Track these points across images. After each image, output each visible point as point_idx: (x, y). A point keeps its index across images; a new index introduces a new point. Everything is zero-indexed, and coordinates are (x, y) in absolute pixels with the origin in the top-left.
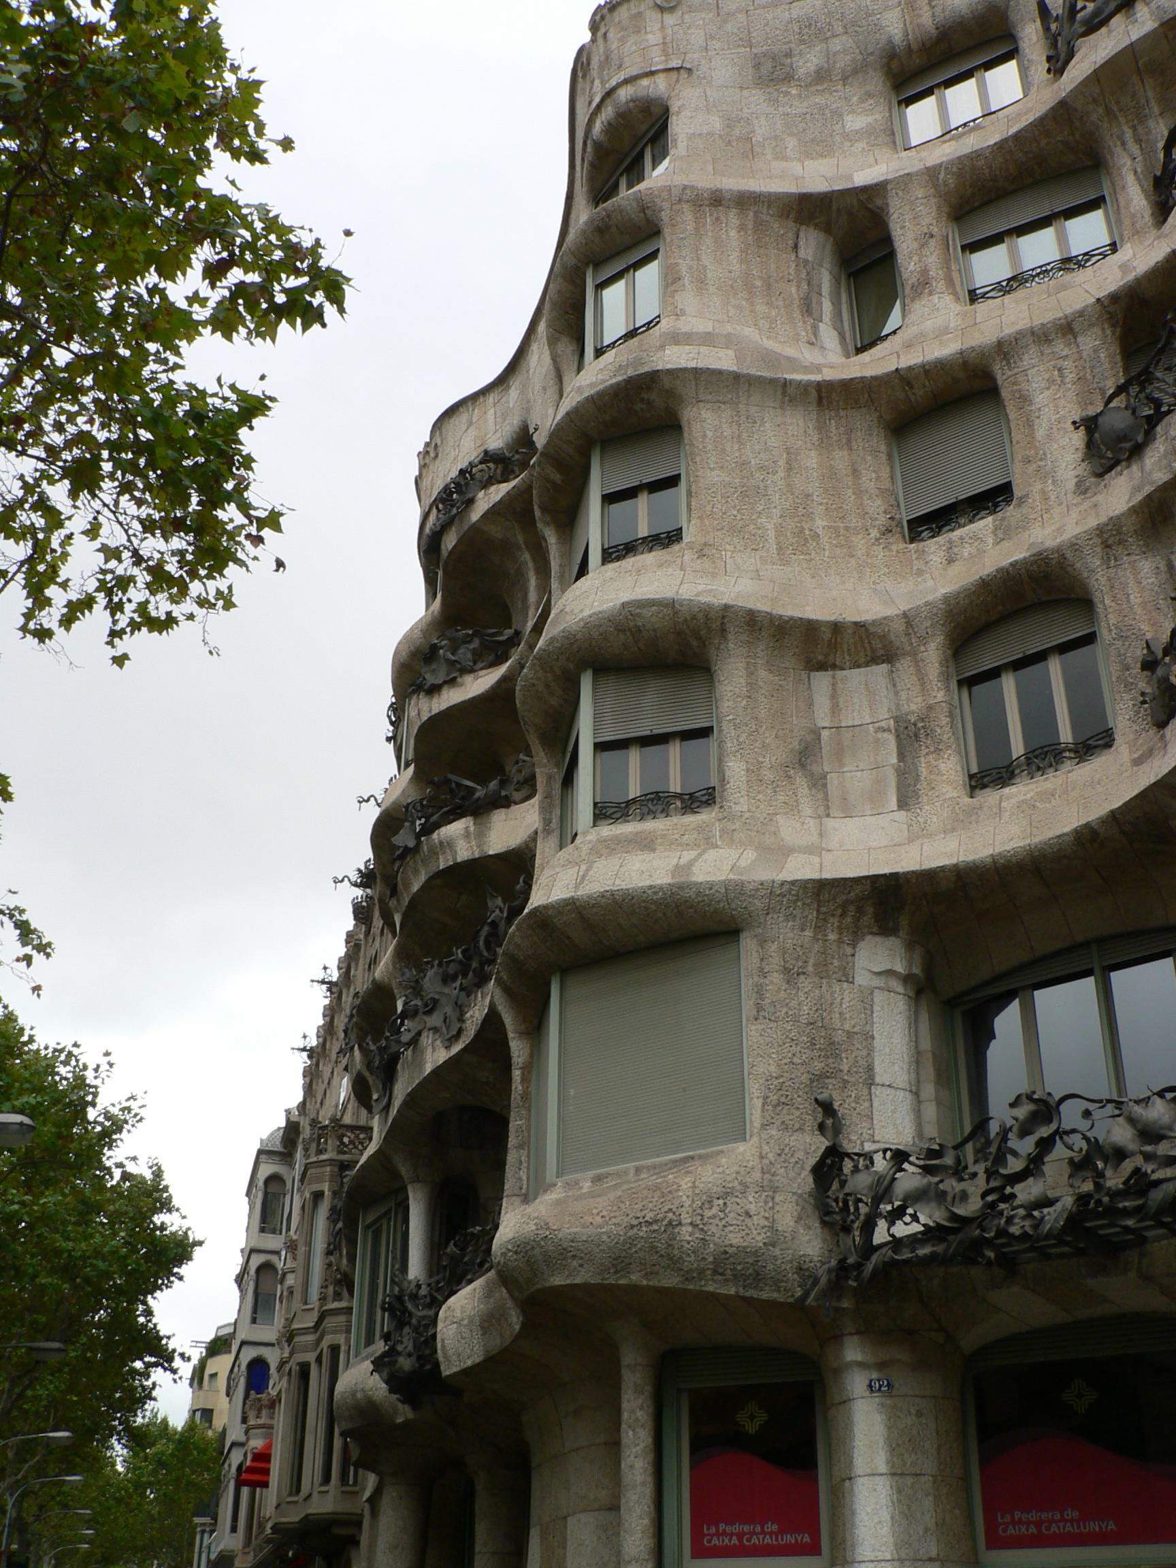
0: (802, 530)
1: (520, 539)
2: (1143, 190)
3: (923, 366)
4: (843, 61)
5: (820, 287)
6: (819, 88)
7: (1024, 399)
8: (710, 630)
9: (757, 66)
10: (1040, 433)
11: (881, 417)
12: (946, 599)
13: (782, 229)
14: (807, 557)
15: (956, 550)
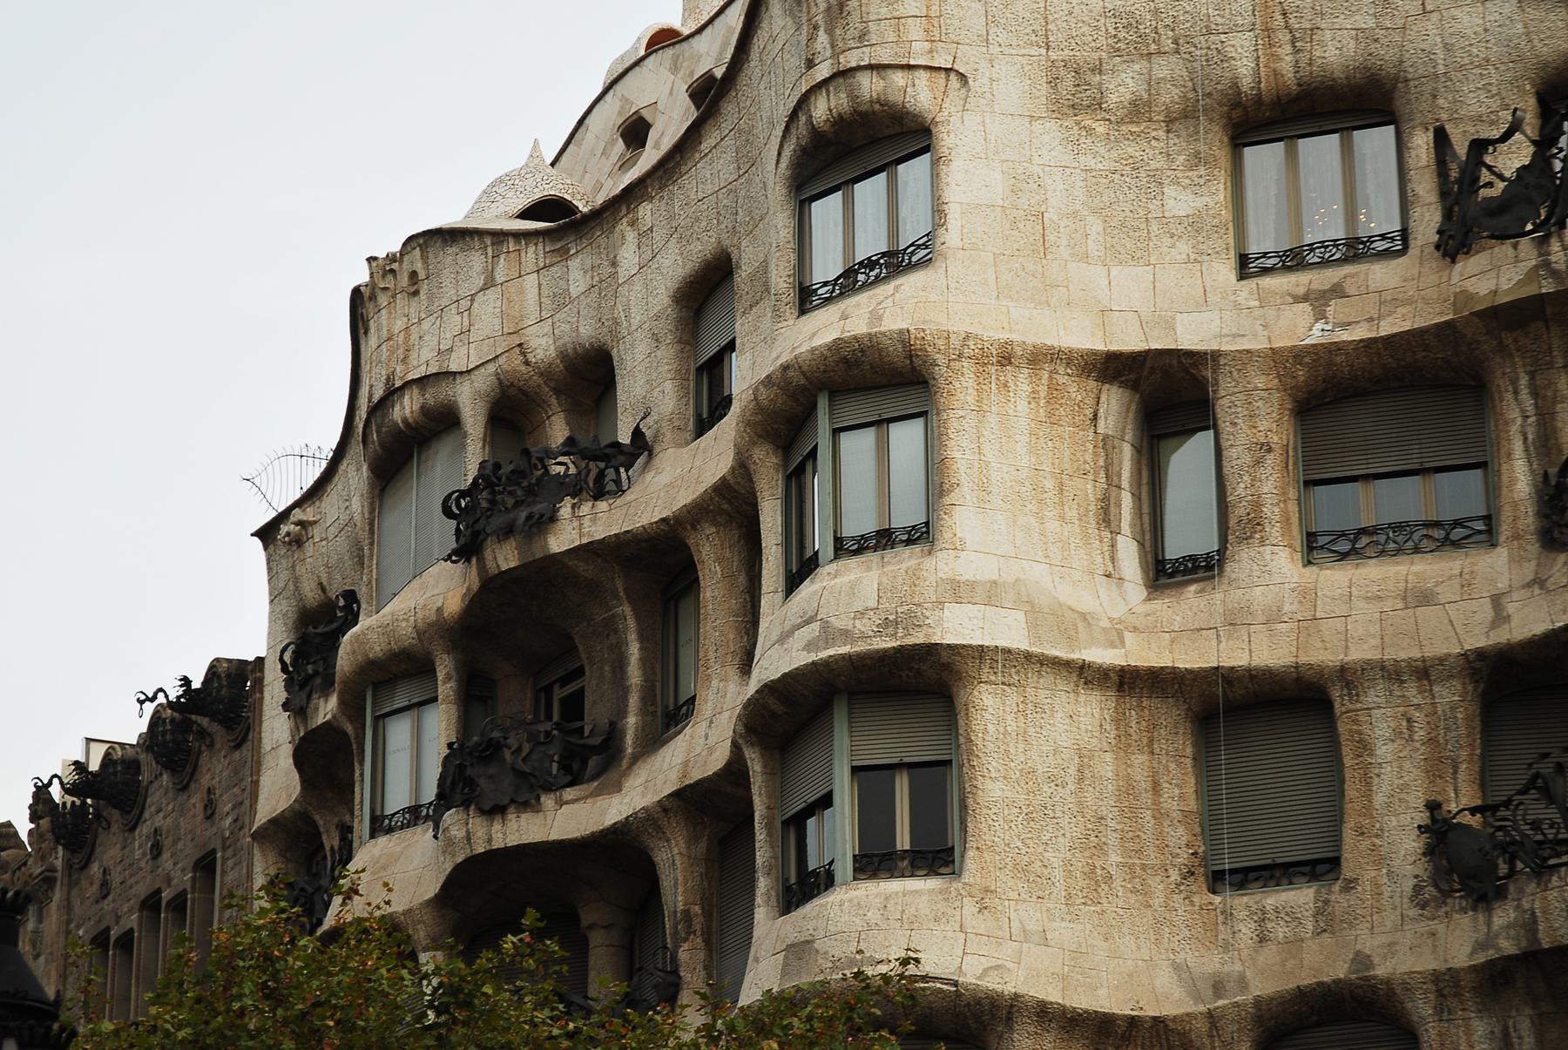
0: (1093, 871)
1: (619, 585)
2: (1532, 471)
3: (1249, 670)
4: (1170, 95)
5: (1119, 475)
6: (1135, 129)
7: (1364, 747)
8: (993, 1017)
9: (1054, 82)
10: (1379, 799)
11: (1189, 709)
12: (1258, 1002)
13: (1077, 390)
14: (1098, 908)
15: (1269, 925)
